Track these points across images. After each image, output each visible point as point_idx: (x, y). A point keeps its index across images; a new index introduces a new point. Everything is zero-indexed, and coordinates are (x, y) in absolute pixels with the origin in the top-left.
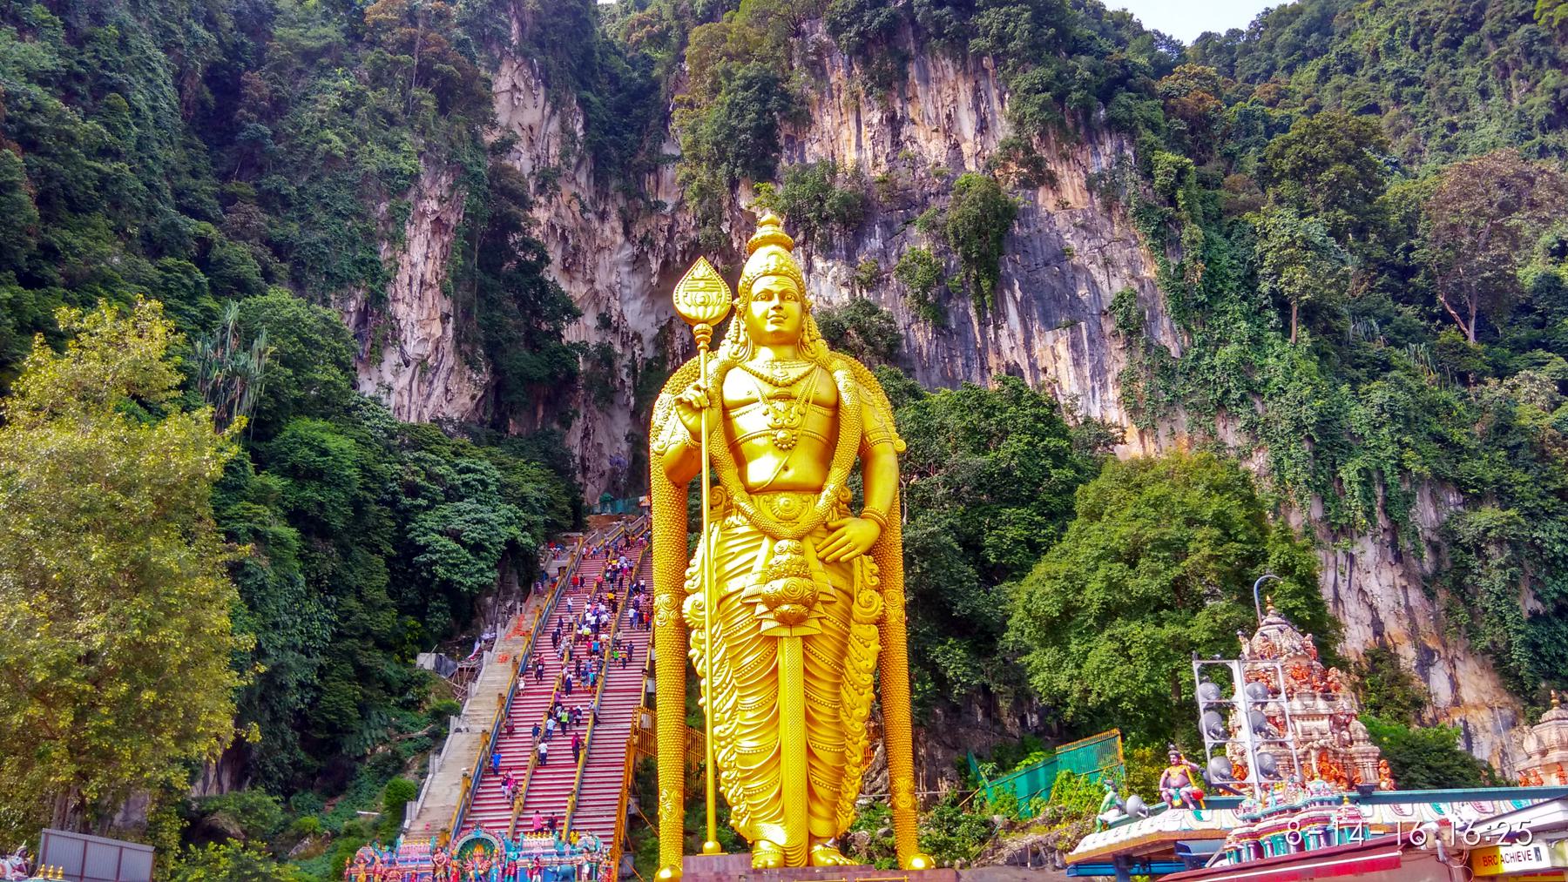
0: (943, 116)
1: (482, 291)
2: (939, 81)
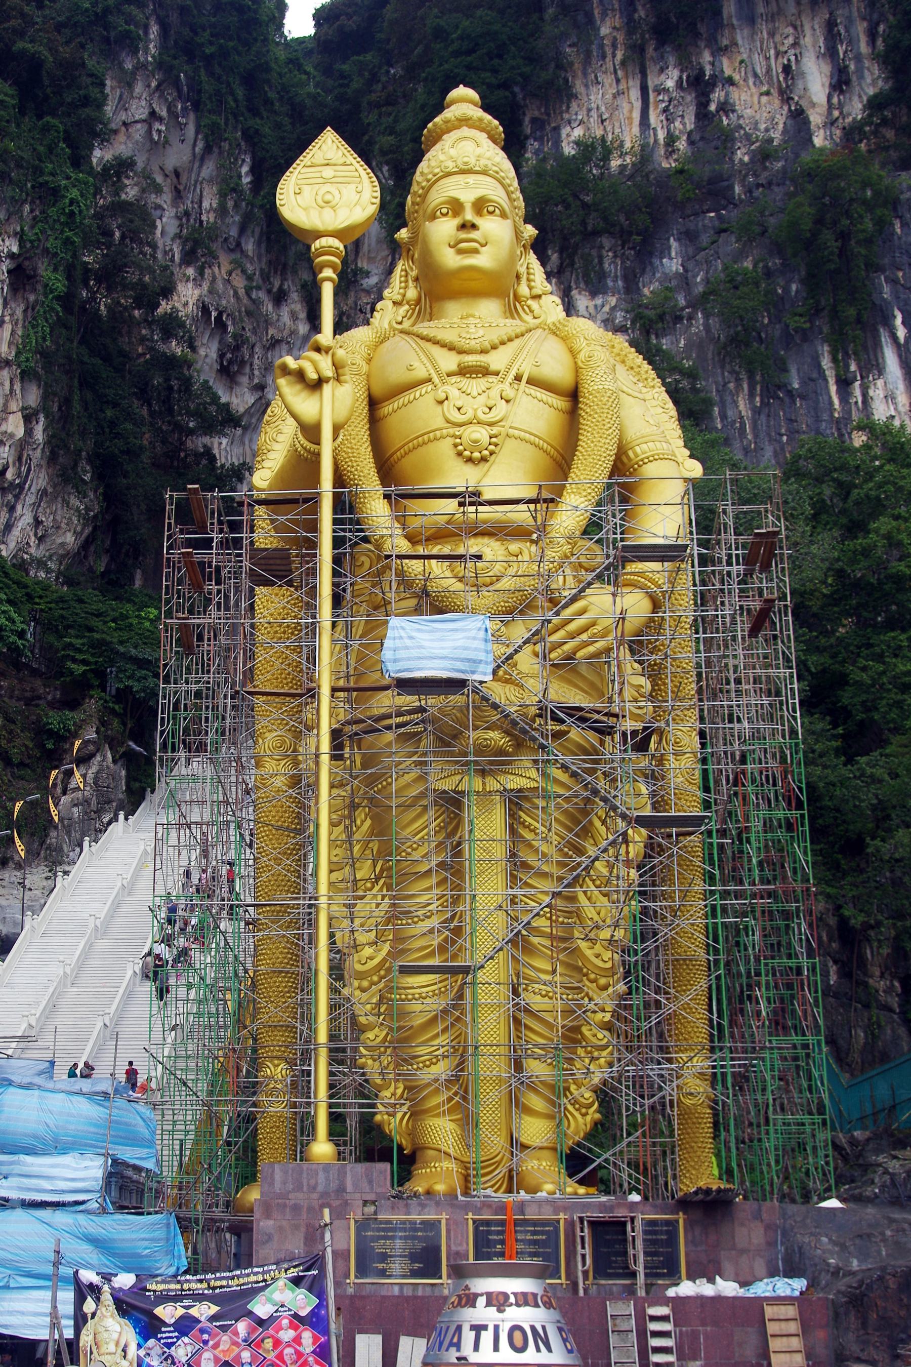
0: (777, 68)
1: (88, 381)
2: (772, 18)
